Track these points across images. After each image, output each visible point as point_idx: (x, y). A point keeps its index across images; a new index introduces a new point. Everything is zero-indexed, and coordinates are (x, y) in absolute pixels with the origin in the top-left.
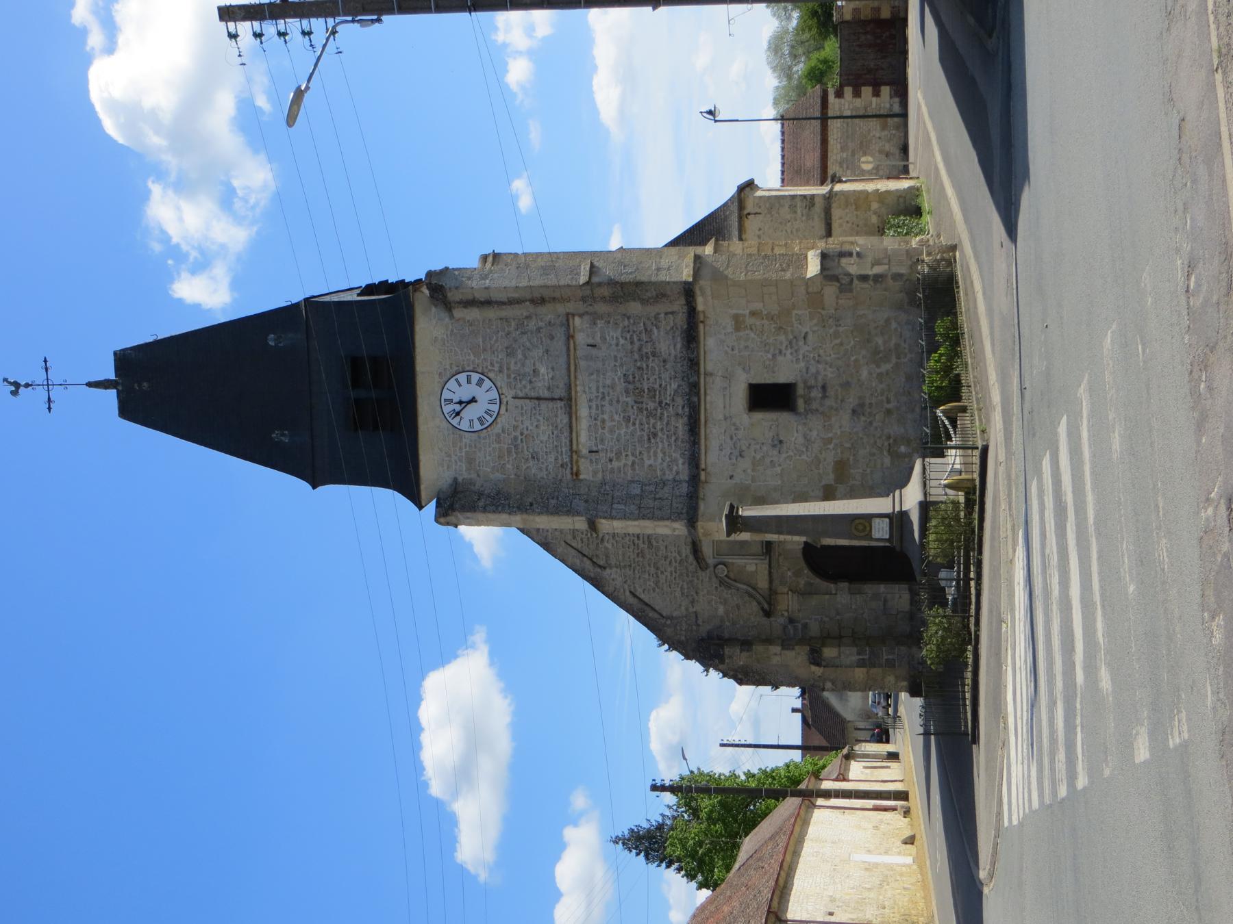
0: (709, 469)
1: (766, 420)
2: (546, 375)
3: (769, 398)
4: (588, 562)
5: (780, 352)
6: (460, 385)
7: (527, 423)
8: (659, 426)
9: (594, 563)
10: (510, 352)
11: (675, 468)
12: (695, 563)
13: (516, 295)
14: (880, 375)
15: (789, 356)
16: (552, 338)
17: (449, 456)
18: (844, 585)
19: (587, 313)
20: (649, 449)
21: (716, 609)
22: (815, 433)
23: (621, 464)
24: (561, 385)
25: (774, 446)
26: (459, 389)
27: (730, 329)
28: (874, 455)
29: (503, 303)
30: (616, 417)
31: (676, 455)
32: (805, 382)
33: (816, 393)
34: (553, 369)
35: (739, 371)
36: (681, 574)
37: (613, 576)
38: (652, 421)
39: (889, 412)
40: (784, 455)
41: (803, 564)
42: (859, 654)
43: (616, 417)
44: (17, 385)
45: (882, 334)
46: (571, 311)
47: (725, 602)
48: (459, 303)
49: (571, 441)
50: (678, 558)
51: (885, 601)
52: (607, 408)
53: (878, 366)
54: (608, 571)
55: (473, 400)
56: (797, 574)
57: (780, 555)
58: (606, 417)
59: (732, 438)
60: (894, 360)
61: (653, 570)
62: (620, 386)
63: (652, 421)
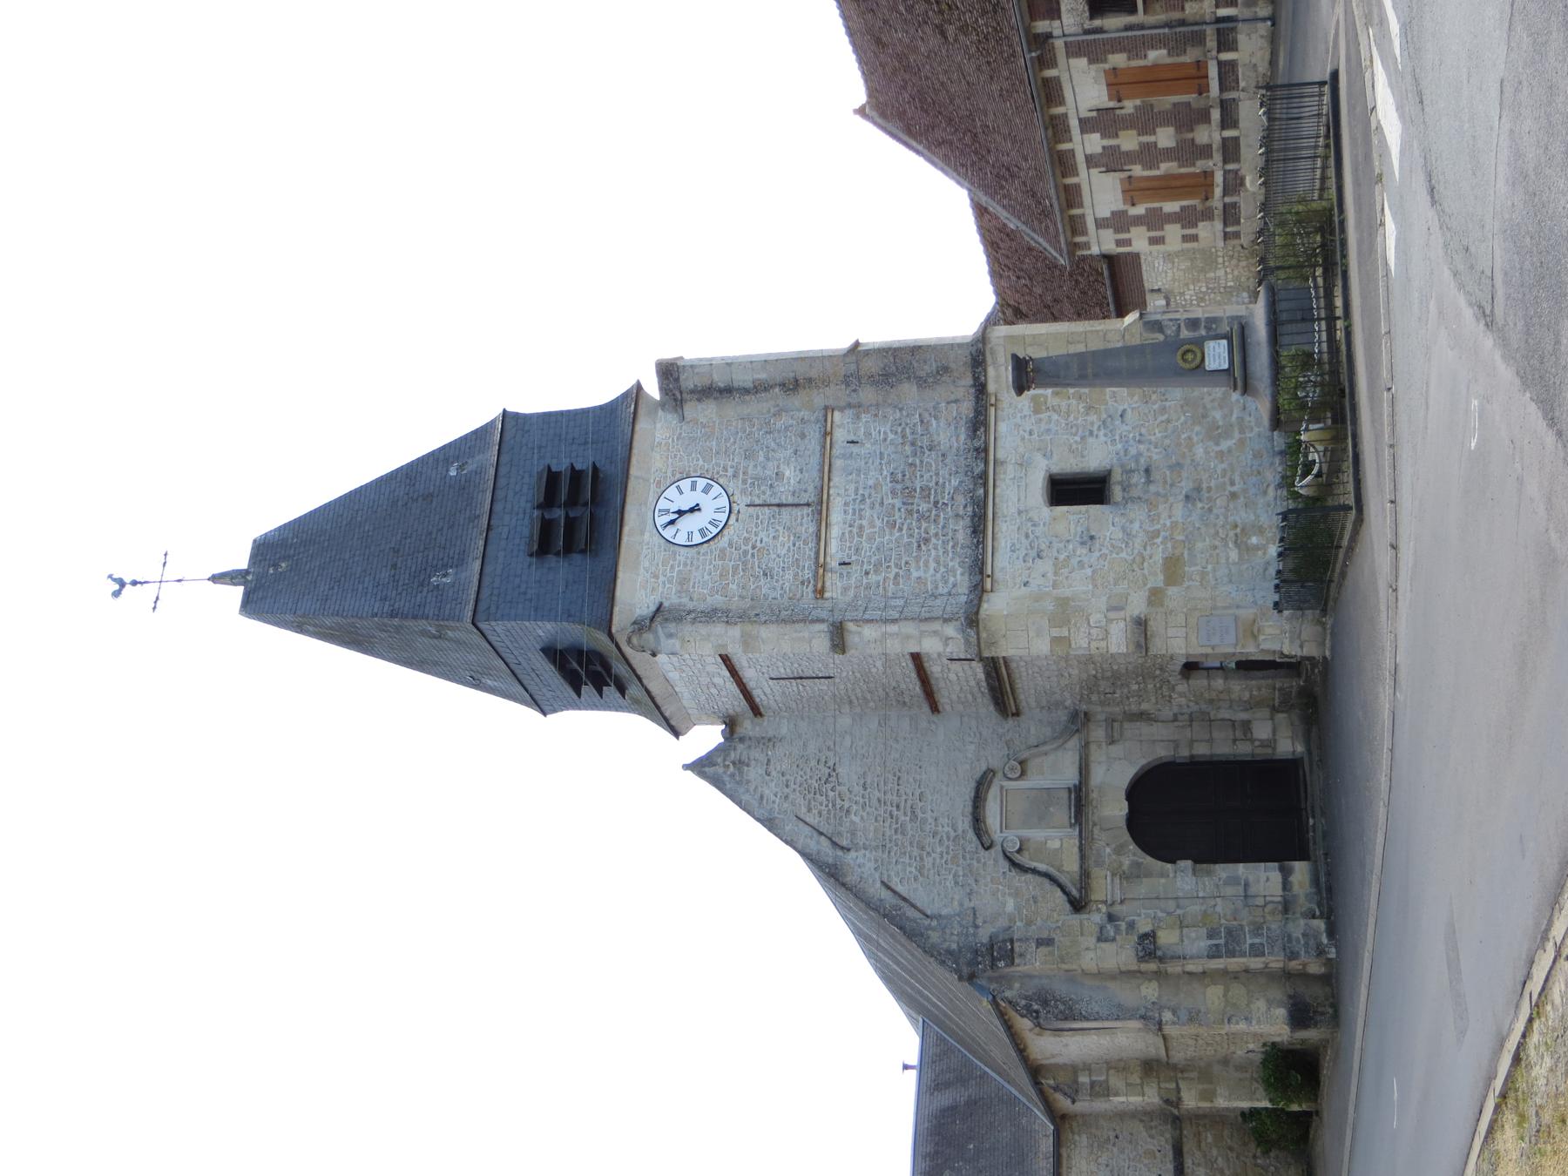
0: (998, 575)
1: (1074, 516)
2: (793, 478)
3: (1071, 490)
4: (824, 842)
5: (1091, 433)
6: (681, 492)
7: (762, 535)
8: (932, 531)
9: (835, 844)
10: (749, 455)
11: (952, 579)
12: (975, 838)
13: (763, 376)
14: (1221, 455)
15: (1102, 439)
16: (803, 436)
17: (656, 577)
18: (1186, 864)
19: (850, 406)
20: (918, 559)
21: (1004, 904)
22: (1136, 525)
23: (880, 578)
24: (811, 488)
25: (1083, 543)
26: (677, 498)
27: (1027, 411)
28: (1216, 548)
29: (746, 391)
30: (878, 523)
31: (954, 564)
32: (1122, 466)
33: (1138, 479)
34: (801, 471)
35: (1038, 457)
36: (955, 856)
37: (860, 860)
38: (924, 525)
39: (1234, 496)
40: (1097, 554)
41: (1127, 837)
42: (1210, 937)
43: (878, 523)
44: (122, 584)
45: (1221, 407)
46: (831, 402)
47: (1016, 894)
48: (692, 392)
49: (817, 553)
50: (953, 834)
51: (1246, 885)
52: (868, 513)
53: (1217, 444)
54: (853, 854)
55: (694, 509)
56: (1119, 850)
57: (1095, 824)
58: (864, 523)
59: (1027, 536)
60: (1237, 435)
61: (916, 852)
62: (887, 487)
63: (924, 525)
